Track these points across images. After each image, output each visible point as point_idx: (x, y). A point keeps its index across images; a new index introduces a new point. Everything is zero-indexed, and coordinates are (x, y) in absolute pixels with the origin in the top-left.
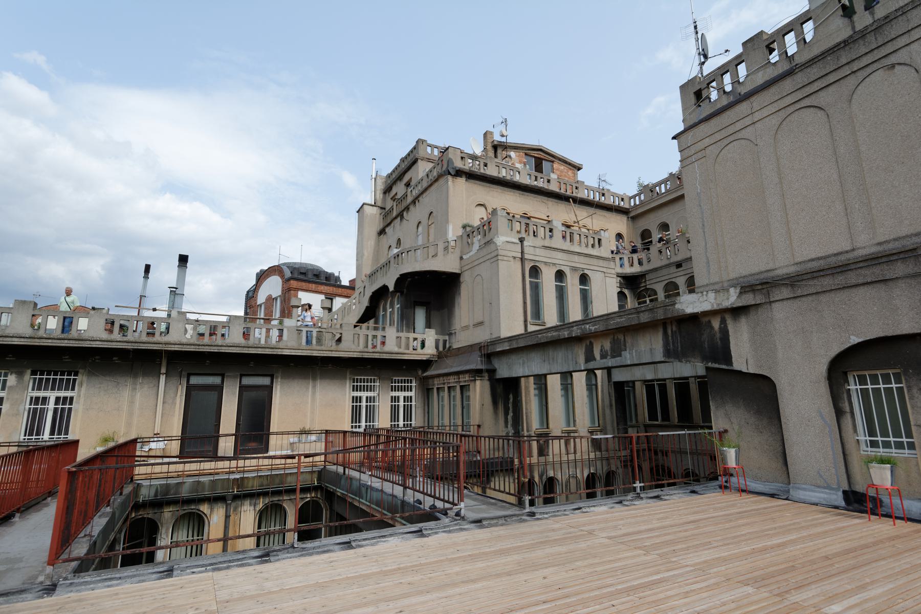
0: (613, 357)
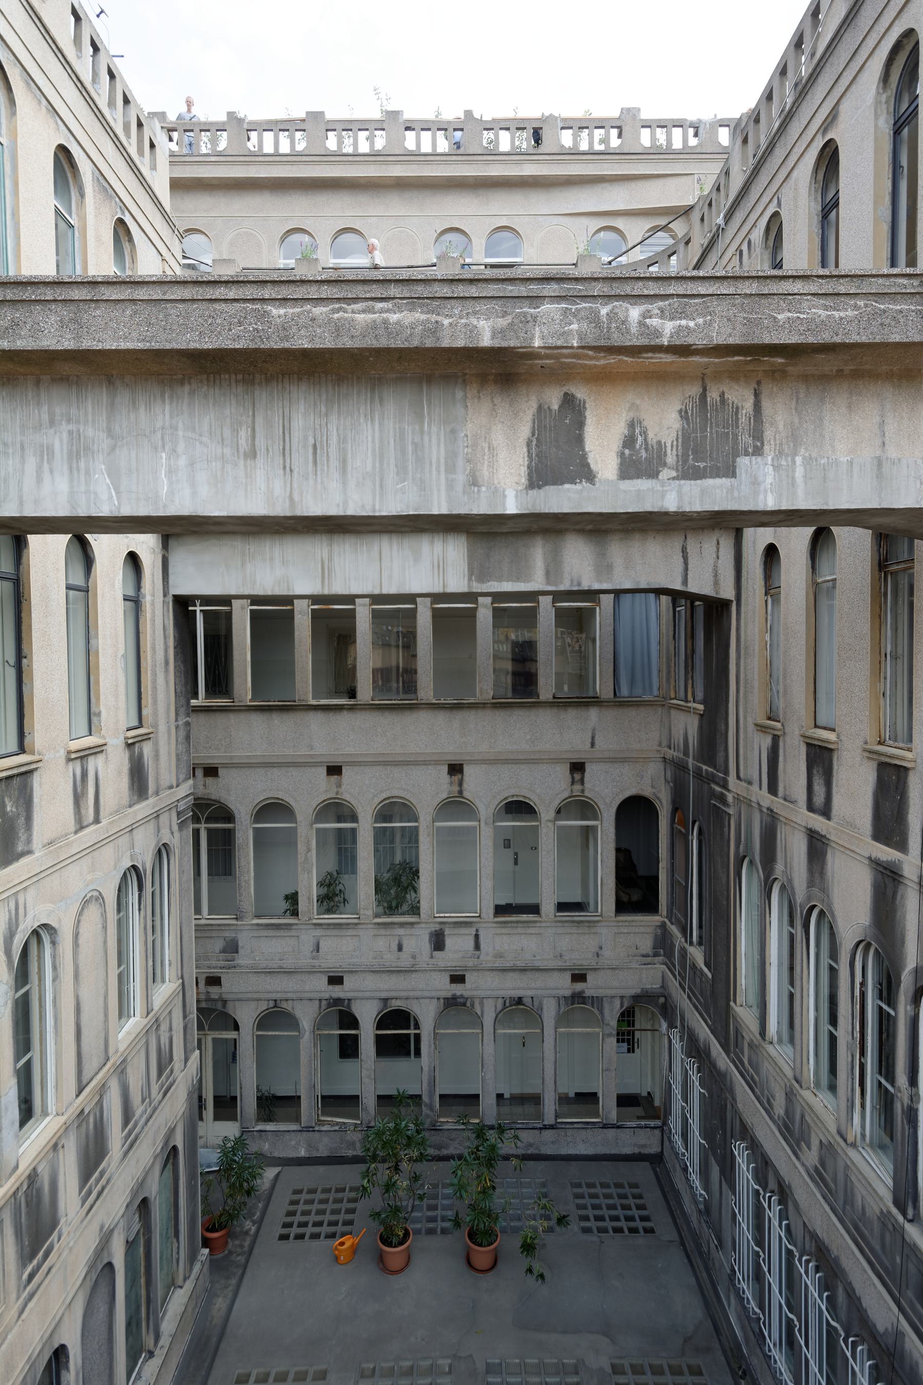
0: (689, 473)
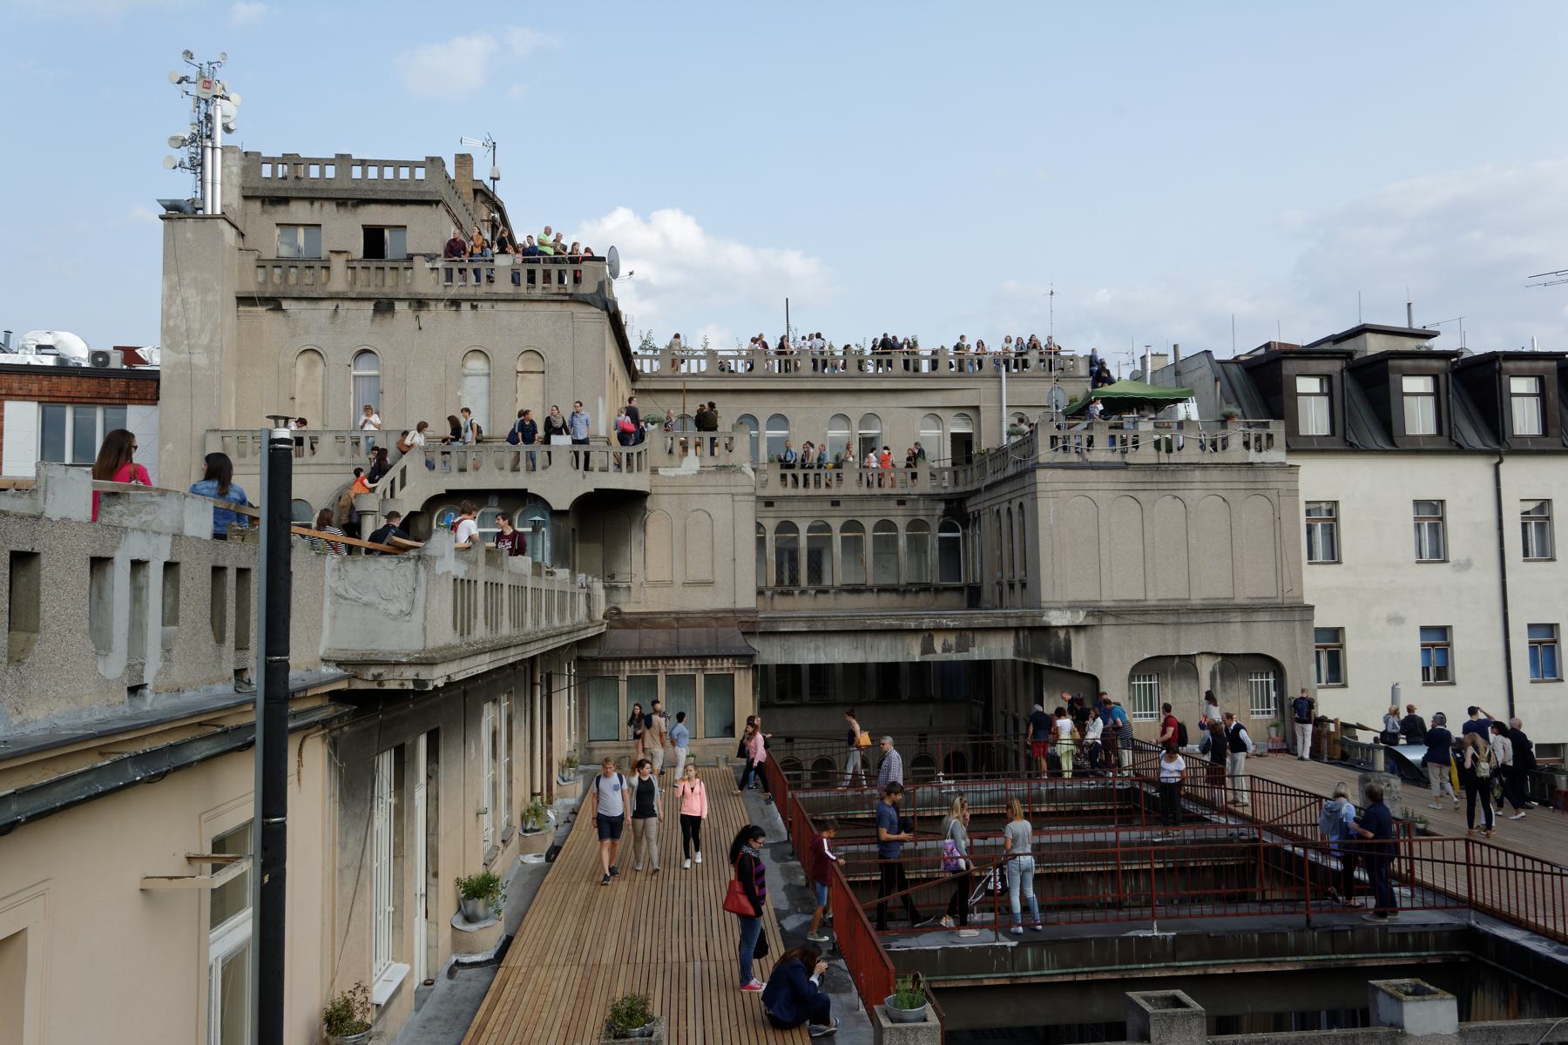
0: (958, 651)
